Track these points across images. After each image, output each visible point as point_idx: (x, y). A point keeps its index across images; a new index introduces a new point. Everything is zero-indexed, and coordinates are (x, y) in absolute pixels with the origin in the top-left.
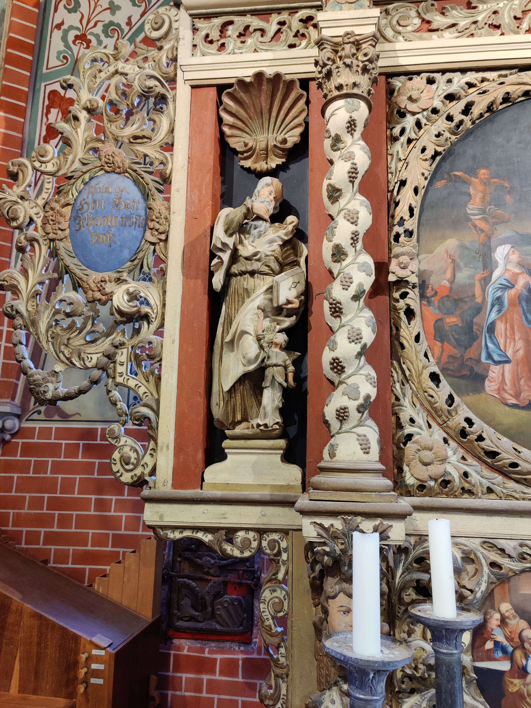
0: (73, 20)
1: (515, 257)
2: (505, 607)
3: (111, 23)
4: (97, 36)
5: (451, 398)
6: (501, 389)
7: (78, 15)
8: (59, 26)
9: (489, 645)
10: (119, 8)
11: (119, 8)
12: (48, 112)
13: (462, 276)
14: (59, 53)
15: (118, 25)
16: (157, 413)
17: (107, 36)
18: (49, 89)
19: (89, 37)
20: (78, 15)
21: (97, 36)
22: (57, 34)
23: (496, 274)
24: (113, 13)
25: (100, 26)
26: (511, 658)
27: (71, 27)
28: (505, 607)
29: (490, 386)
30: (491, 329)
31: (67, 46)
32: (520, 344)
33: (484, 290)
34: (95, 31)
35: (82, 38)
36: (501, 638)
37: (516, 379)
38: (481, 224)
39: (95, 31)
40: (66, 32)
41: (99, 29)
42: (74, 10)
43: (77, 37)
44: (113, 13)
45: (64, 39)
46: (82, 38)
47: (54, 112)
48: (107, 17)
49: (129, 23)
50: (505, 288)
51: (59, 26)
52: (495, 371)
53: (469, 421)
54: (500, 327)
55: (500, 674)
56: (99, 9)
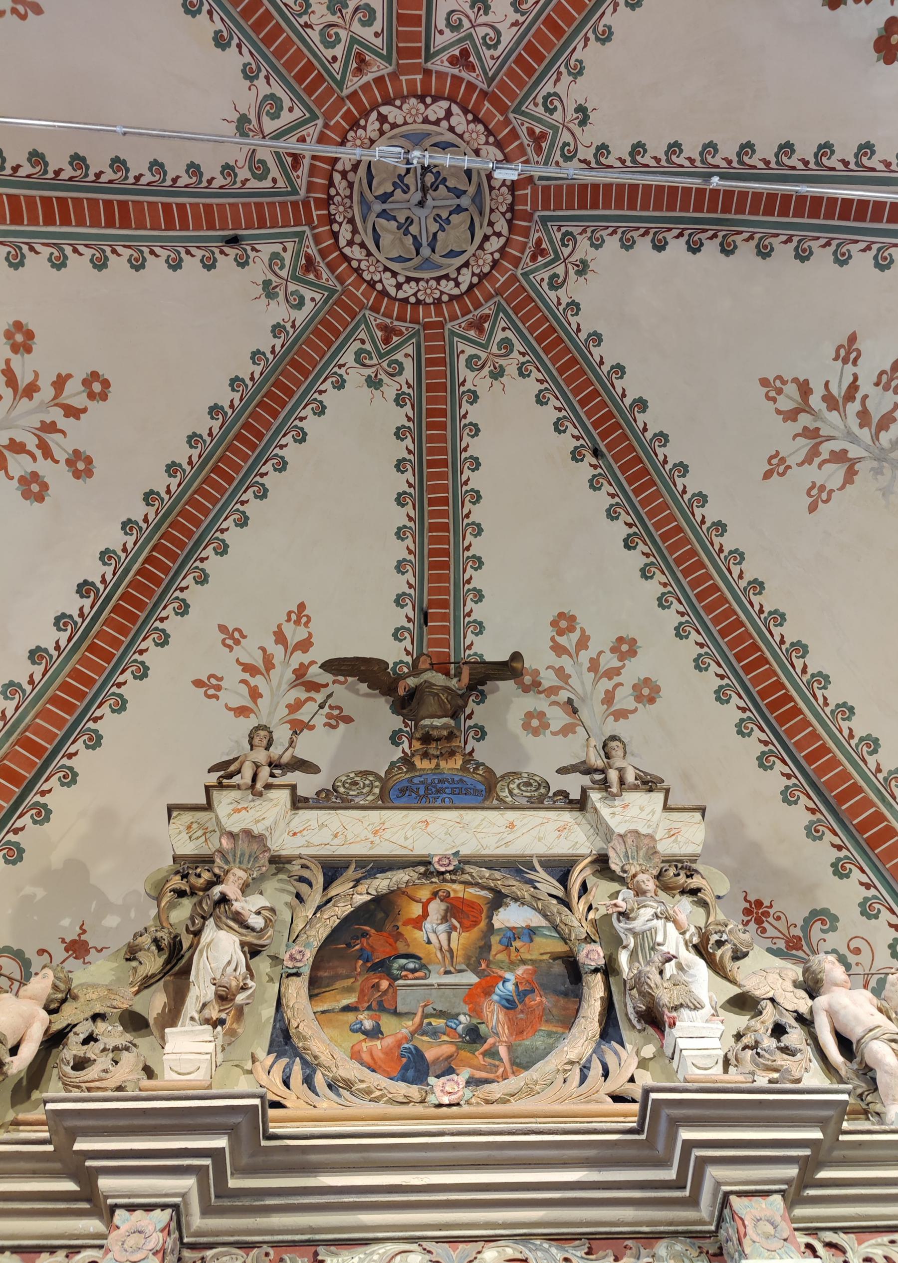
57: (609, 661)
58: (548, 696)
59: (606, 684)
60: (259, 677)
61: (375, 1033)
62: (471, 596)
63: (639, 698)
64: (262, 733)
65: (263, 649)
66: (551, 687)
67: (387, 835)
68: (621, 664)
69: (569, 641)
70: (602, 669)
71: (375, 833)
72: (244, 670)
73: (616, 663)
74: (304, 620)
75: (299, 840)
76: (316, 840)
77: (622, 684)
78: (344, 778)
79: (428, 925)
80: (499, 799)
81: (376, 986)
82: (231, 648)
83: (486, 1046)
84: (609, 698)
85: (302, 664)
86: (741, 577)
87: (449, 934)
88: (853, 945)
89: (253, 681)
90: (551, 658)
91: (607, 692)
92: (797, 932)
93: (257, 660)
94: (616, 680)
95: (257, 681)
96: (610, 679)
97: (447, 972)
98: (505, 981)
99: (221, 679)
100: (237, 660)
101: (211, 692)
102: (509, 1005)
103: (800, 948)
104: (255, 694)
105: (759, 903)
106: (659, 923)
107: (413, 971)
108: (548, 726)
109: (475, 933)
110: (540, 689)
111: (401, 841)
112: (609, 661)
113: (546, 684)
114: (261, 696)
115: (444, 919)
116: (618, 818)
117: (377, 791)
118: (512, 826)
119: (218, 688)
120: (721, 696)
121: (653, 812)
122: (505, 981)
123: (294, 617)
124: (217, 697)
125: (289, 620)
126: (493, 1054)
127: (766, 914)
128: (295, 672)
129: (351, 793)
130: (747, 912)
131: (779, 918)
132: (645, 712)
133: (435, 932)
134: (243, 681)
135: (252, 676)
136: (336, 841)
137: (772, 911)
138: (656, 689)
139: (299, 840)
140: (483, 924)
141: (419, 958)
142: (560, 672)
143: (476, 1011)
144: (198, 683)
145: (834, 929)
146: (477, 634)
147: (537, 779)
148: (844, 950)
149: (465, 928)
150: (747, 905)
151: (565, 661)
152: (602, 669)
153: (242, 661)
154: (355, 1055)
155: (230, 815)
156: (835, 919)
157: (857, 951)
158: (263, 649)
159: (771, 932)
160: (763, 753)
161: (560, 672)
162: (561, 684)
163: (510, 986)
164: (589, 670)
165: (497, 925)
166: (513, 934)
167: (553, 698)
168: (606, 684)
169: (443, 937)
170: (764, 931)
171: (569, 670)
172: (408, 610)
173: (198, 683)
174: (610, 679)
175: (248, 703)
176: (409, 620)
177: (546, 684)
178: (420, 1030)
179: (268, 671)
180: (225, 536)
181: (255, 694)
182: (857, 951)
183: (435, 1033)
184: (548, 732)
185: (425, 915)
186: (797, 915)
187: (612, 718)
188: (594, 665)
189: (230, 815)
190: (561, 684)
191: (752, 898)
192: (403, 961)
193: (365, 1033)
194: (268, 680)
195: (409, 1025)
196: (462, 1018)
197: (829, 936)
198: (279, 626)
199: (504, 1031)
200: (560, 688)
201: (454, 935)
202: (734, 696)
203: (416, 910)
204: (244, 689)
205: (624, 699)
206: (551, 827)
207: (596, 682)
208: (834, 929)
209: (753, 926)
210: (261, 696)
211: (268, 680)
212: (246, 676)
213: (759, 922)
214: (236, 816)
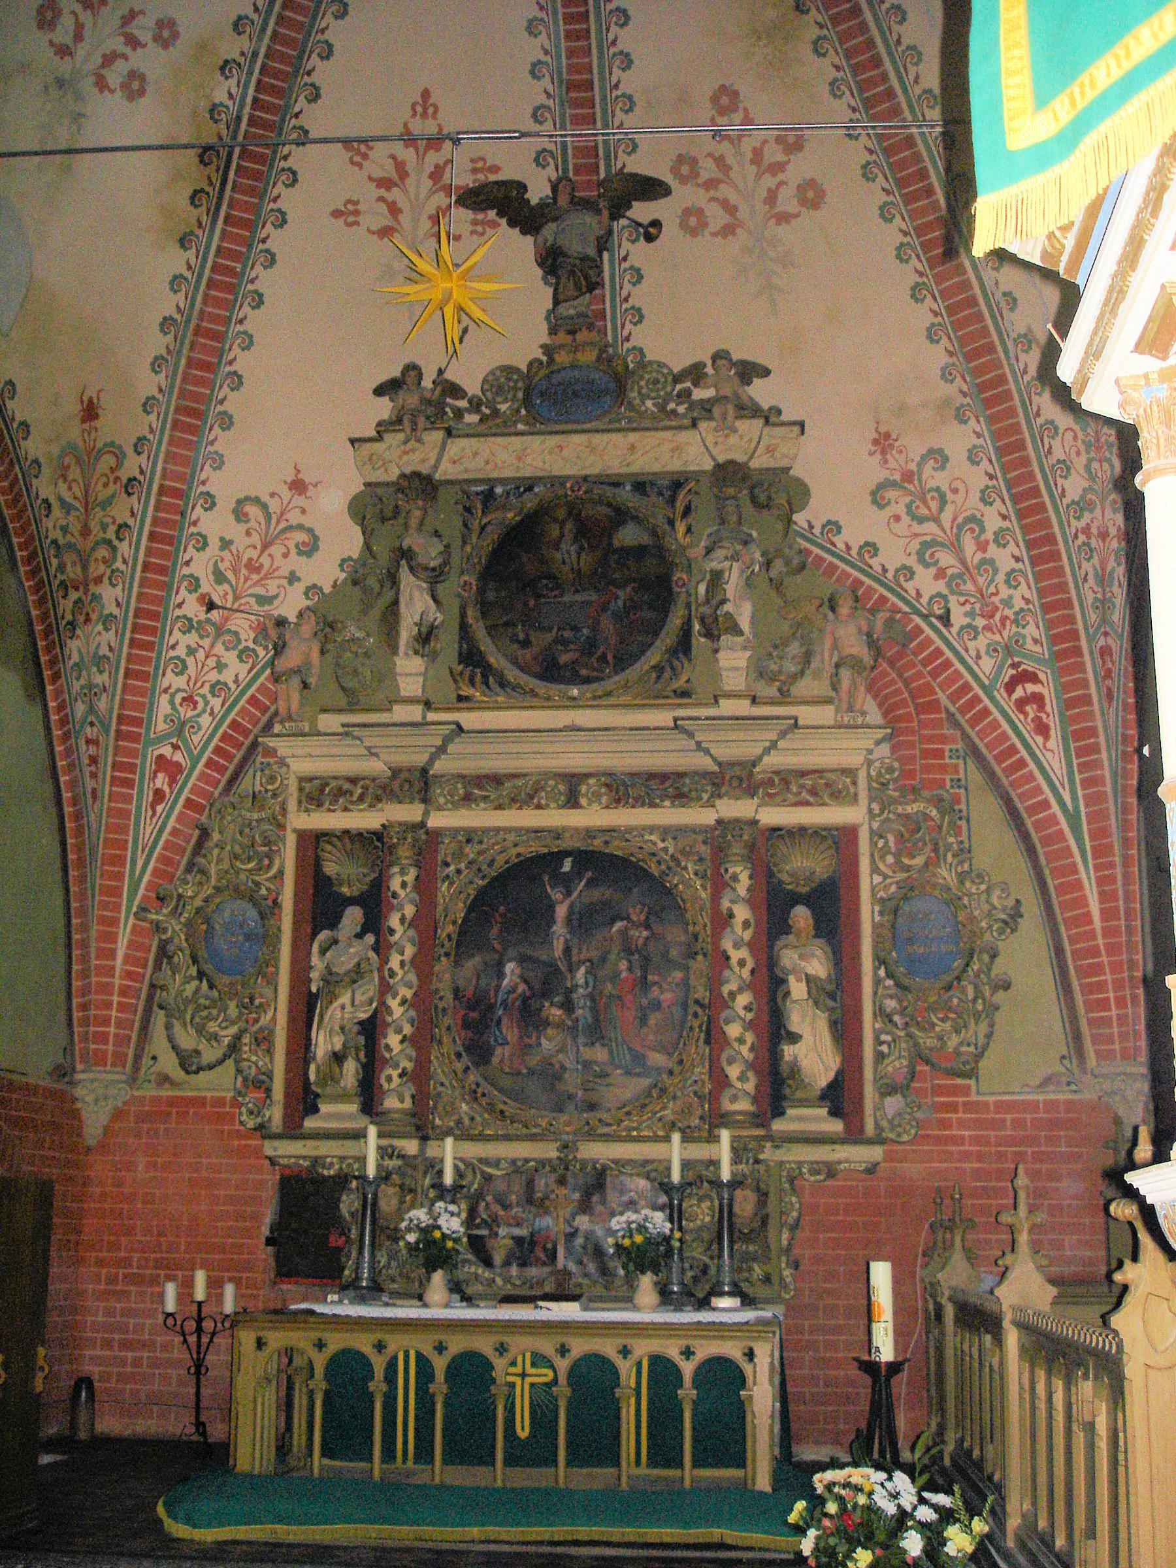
0: (180, 682)
1: (518, 971)
2: (489, 1198)
3: (218, 682)
4: (204, 697)
5: (468, 1068)
6: (502, 1061)
7: (185, 677)
8: (166, 691)
9: (478, 1221)
10: (226, 666)
11: (226, 666)
12: (155, 776)
13: (483, 982)
14: (166, 717)
15: (226, 684)
16: (271, 1078)
17: (214, 695)
18: (156, 753)
19: (197, 698)
20: (185, 677)
21: (204, 697)
22: (165, 699)
23: (505, 982)
24: (220, 672)
25: (207, 687)
26: (491, 1229)
27: (178, 690)
28: (489, 1198)
29: (495, 1060)
30: (499, 1022)
31: (174, 708)
32: (516, 1030)
33: (496, 995)
34: (201, 691)
35: (189, 700)
36: (484, 1216)
37: (511, 1055)
38: (498, 947)
39: (201, 691)
40: (173, 696)
41: (206, 690)
42: (181, 673)
43: (184, 699)
44: (220, 672)
45: (172, 702)
46: (189, 700)
47: (160, 776)
48: (214, 676)
49: (236, 681)
50: (509, 992)
51: (166, 691)
52: (498, 1051)
53: (478, 1085)
54: (505, 1021)
55: (482, 1237)
56: (206, 669)
57: (774, 154)
58: (707, 190)
59: (768, 181)
60: (395, 190)
61: (526, 644)
62: (618, 63)
63: (803, 202)
64: (413, 374)
65: (393, 157)
66: (711, 180)
67: (529, 460)
68: (785, 159)
69: (731, 125)
70: (766, 162)
71: (519, 459)
72: (378, 186)
73: (780, 157)
74: (431, 110)
75: (459, 468)
76: (472, 466)
77: (785, 183)
78: (491, 378)
79: (563, 546)
80: (630, 403)
81: (526, 604)
82: (360, 165)
83: (599, 653)
84: (772, 197)
85: (437, 166)
86: (916, 81)
87: (579, 554)
88: (956, 484)
89: (390, 196)
90: (710, 145)
91: (770, 190)
92: (913, 467)
93: (390, 171)
94: (780, 177)
95: (395, 195)
96: (774, 175)
97: (577, 591)
98: (617, 598)
99: (356, 203)
100: (370, 178)
101: (351, 219)
102: (617, 617)
103: (910, 482)
104: (394, 210)
105: (887, 436)
106: (727, 564)
107: (552, 590)
108: (706, 225)
109: (598, 553)
110: (700, 180)
111: (540, 465)
112: (774, 154)
113: (704, 176)
114: (401, 211)
115: (576, 540)
116: (720, 447)
117: (520, 395)
118: (632, 448)
119: (356, 213)
120: (885, 212)
121: (750, 440)
122: (617, 598)
123: (419, 109)
124: (357, 223)
125: (415, 114)
126: (603, 659)
127: (891, 446)
128: (431, 176)
129: (499, 399)
130: (876, 442)
131: (901, 452)
132: (808, 218)
133: (568, 552)
134: (381, 199)
135: (388, 189)
136: (488, 467)
137: (897, 444)
138: (821, 194)
139: (459, 468)
140: (605, 543)
141: (555, 578)
142: (720, 161)
143: (595, 628)
144: (336, 214)
145: (943, 468)
146: (627, 112)
147: (665, 371)
148: (945, 488)
149: (593, 548)
150: (876, 436)
151: (725, 148)
152: (766, 162)
153: (374, 176)
154: (515, 662)
155: (400, 457)
156: (946, 460)
157: (955, 491)
158: (393, 157)
159: (892, 464)
160: (917, 284)
161: (720, 161)
162: (721, 176)
163: (620, 603)
164: (752, 162)
165: (616, 543)
166: (626, 552)
167: (712, 193)
168: (768, 181)
169: (574, 556)
170: (886, 462)
171: (731, 160)
172: (546, 82)
173: (336, 214)
174: (774, 175)
175: (390, 222)
176: (549, 96)
177: (704, 176)
178: (556, 641)
179: (402, 179)
180: (327, 36)
181: (394, 210)
182: (955, 491)
183: (565, 642)
184: (706, 232)
185: (562, 535)
186: (916, 450)
187: (773, 221)
188: (757, 154)
189: (400, 457)
190: (721, 176)
191: (883, 429)
192: (545, 582)
193: (518, 642)
194: (405, 191)
195: (549, 637)
196: (585, 631)
197: (938, 474)
198: (405, 125)
199: (613, 640)
200: (720, 181)
201: (583, 556)
202: (898, 216)
203: (555, 531)
204: (383, 208)
205: (787, 201)
206: (666, 448)
207: (759, 176)
208: (943, 468)
209: (878, 456)
210: (401, 211)
211: (405, 191)
212: (382, 192)
213: (883, 453)
214: (405, 458)
